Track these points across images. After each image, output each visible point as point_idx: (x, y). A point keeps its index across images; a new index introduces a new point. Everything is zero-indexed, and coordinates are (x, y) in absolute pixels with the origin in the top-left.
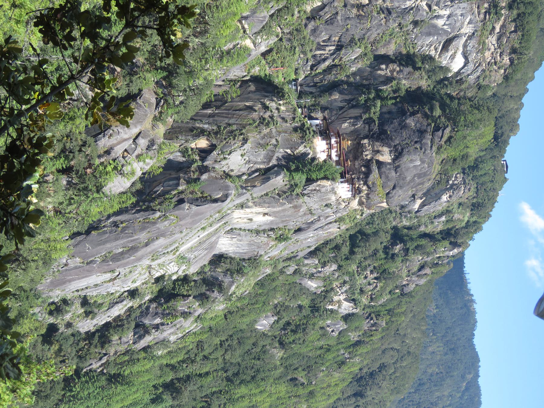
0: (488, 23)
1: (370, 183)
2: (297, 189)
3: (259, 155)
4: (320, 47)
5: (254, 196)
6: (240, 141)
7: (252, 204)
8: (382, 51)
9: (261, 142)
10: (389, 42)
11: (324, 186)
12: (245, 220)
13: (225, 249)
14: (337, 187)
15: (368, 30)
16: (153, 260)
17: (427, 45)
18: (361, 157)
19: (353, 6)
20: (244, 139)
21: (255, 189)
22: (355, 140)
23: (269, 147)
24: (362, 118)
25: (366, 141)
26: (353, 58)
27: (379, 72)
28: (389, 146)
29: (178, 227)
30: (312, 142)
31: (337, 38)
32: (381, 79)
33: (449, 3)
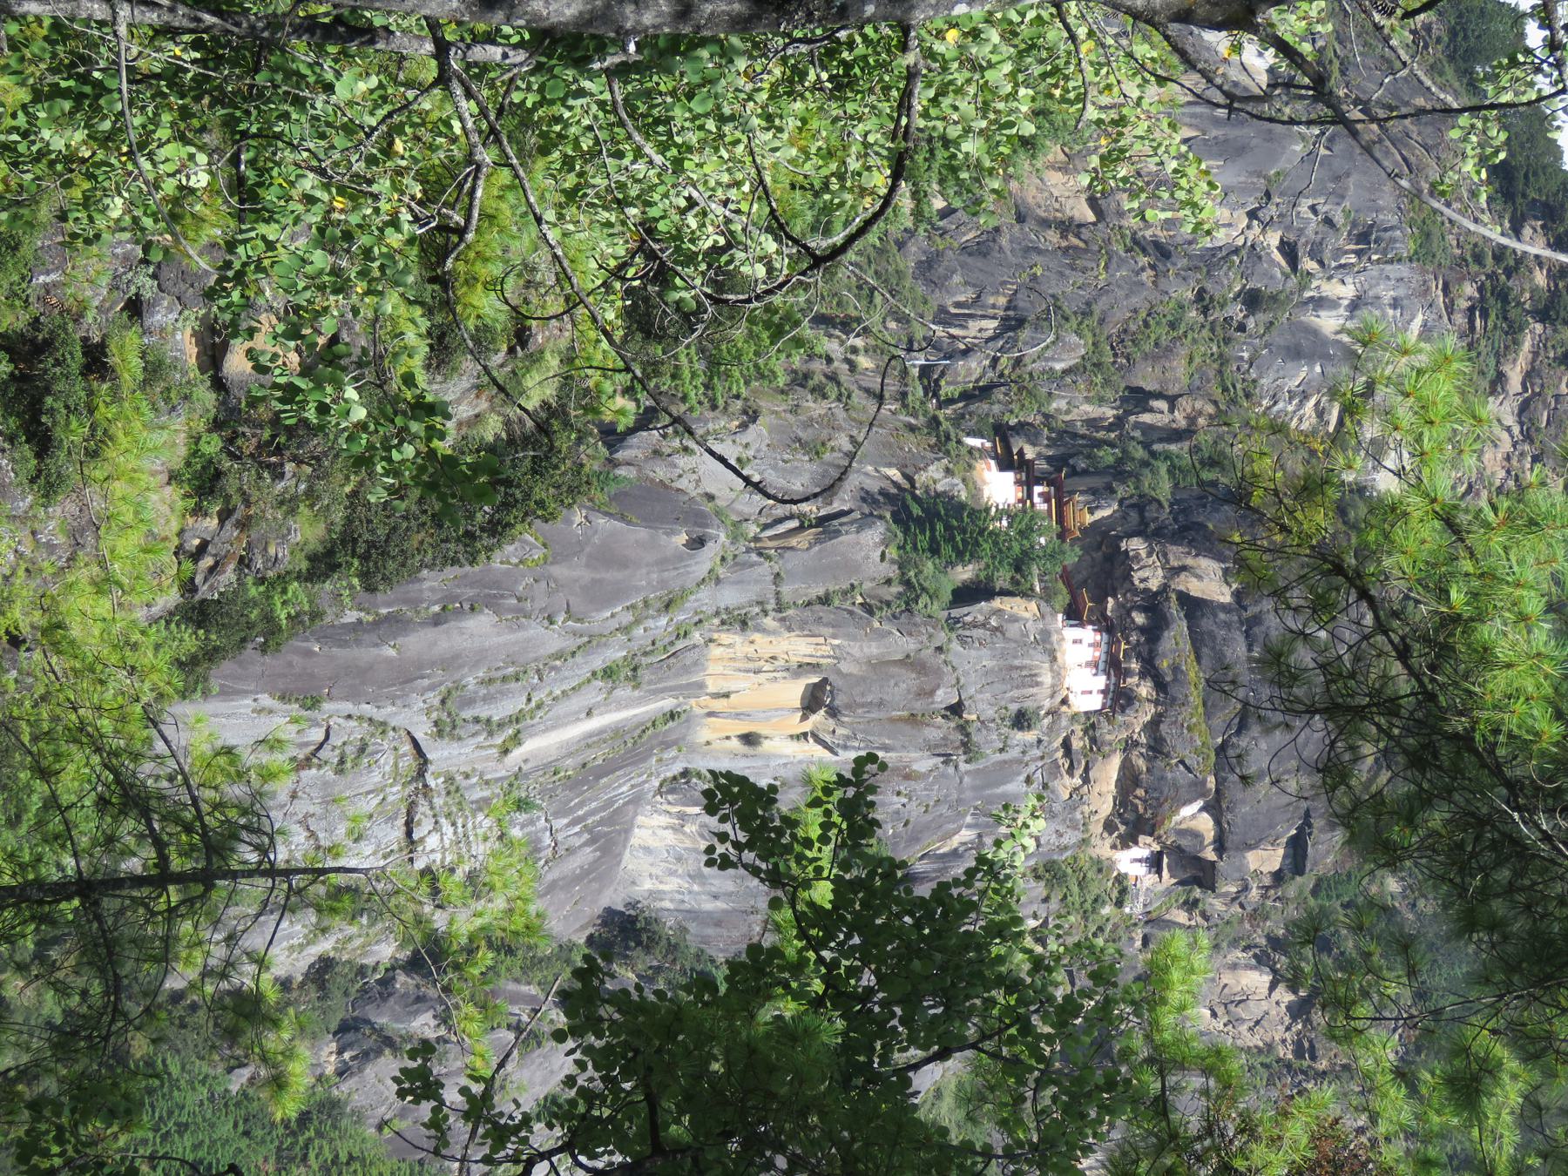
0: (1483, 342)
1: (1164, 664)
2: (924, 599)
3: (795, 472)
4: (943, 317)
5: (786, 590)
6: (731, 417)
7: (775, 624)
8: (1146, 378)
9: (801, 434)
10: (1169, 350)
11: (1014, 619)
12: (735, 744)
13: (648, 885)
14: (1059, 632)
15: (1102, 291)
16: (440, 730)
17: (1294, 396)
18: (1127, 585)
19: (1045, 223)
20: (745, 412)
21: (788, 554)
22: (1099, 547)
23: (827, 456)
24: (1113, 491)
25: (1136, 545)
26: (1059, 366)
27: (1146, 418)
28: (1220, 558)
29: (543, 584)
30: (970, 466)
31: (1002, 301)
32: (1155, 436)
33: (1353, 259)
